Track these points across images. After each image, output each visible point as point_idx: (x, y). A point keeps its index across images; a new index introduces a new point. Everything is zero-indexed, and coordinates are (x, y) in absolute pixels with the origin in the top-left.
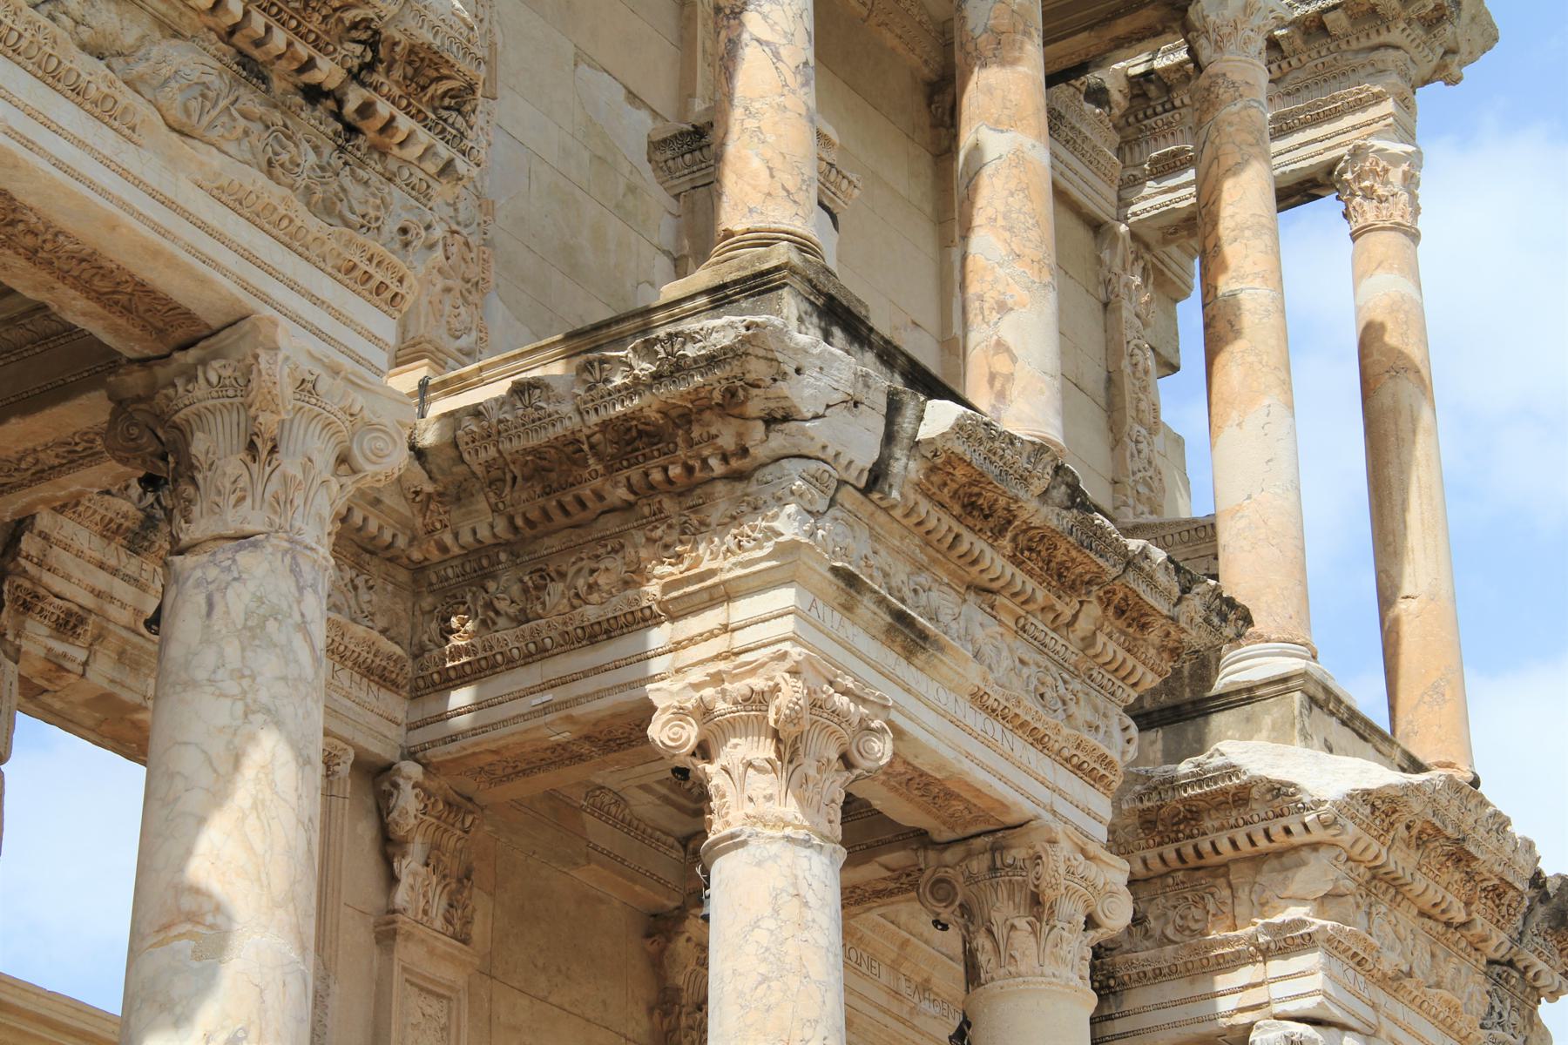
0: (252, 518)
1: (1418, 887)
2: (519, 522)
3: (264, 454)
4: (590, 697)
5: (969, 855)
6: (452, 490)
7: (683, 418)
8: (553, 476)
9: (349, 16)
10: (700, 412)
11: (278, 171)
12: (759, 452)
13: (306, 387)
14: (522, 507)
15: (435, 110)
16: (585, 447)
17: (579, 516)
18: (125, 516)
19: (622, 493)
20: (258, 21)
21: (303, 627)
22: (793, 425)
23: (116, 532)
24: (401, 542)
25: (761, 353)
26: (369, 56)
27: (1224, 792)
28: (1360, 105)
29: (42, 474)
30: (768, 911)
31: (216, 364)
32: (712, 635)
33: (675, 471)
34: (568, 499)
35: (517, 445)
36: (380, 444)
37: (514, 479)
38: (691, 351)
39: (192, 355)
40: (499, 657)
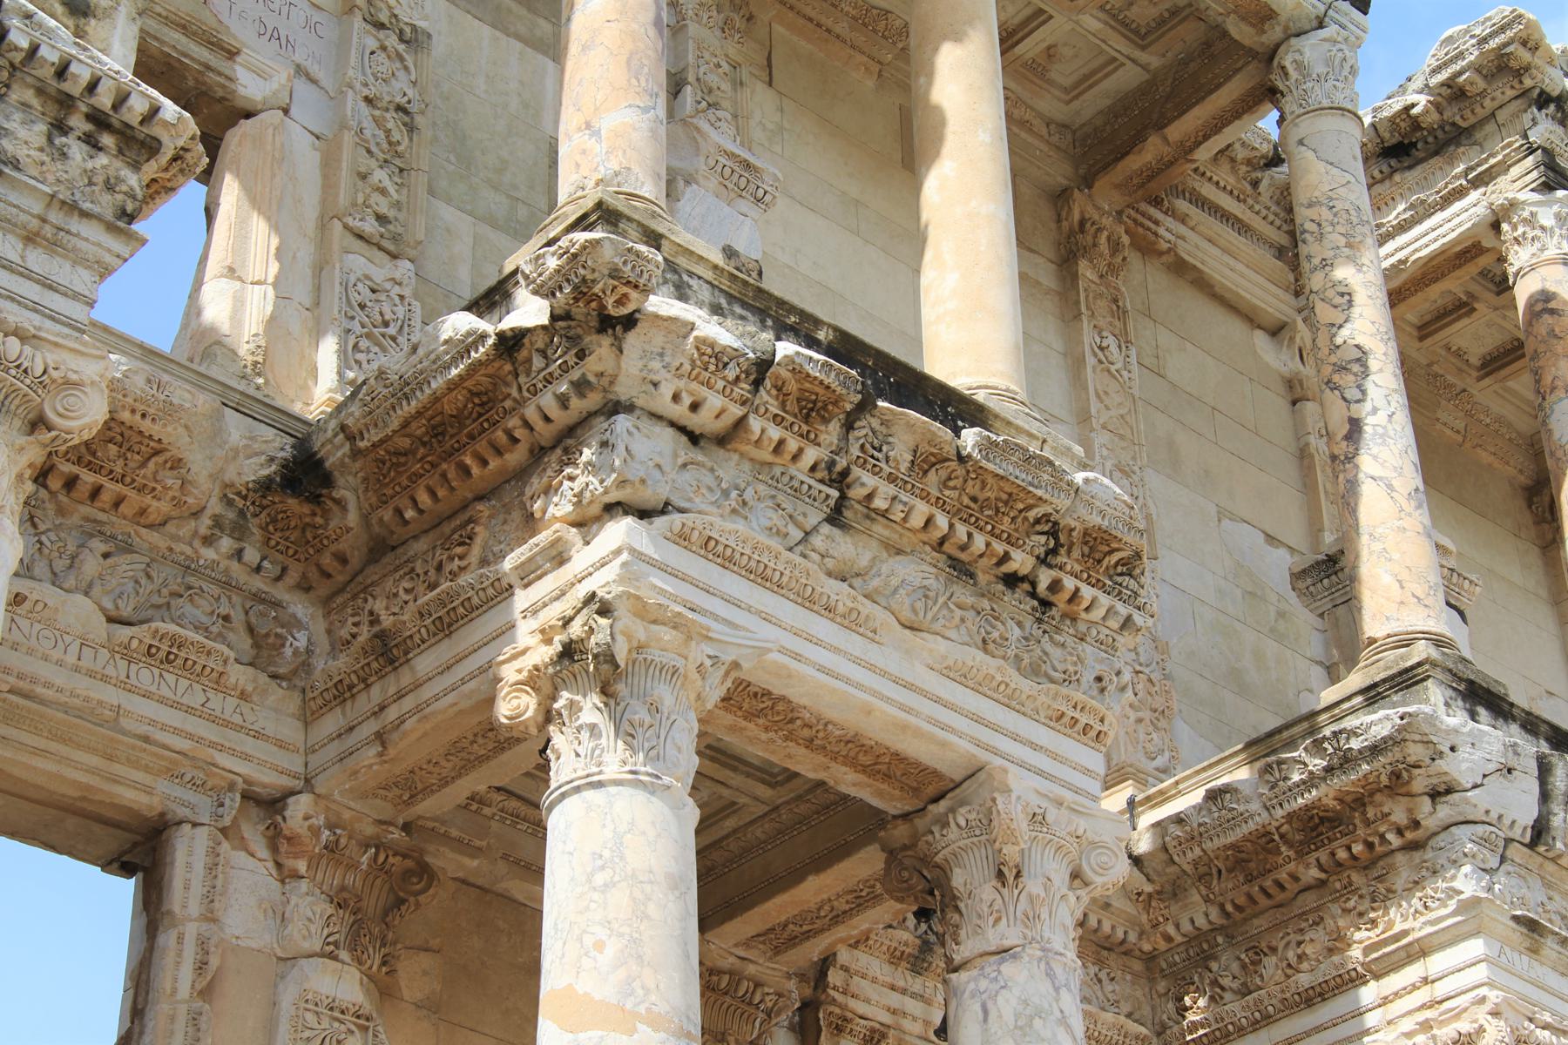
0: (1009, 934)
2: (1229, 908)
3: (1011, 880)
6: (1168, 888)
7: (1358, 802)
8: (1252, 865)
9: (1032, 515)
10: (1372, 794)
11: (991, 646)
12: (1430, 823)
13: (1038, 819)
14: (1230, 895)
15: (1110, 578)
16: (1276, 837)
17: (1280, 897)
18: (906, 944)
19: (1314, 873)
20: (961, 530)
21: (1063, 1021)
22: (1456, 796)
23: (900, 958)
24: (1132, 937)
25: (1417, 738)
26: (1052, 544)
29: (837, 919)
31: (963, 810)
32: (1414, 987)
33: (1357, 848)
34: (1268, 883)
35: (1218, 843)
36: (1104, 859)
38: (1355, 744)
39: (943, 805)
40: (1230, 1027)
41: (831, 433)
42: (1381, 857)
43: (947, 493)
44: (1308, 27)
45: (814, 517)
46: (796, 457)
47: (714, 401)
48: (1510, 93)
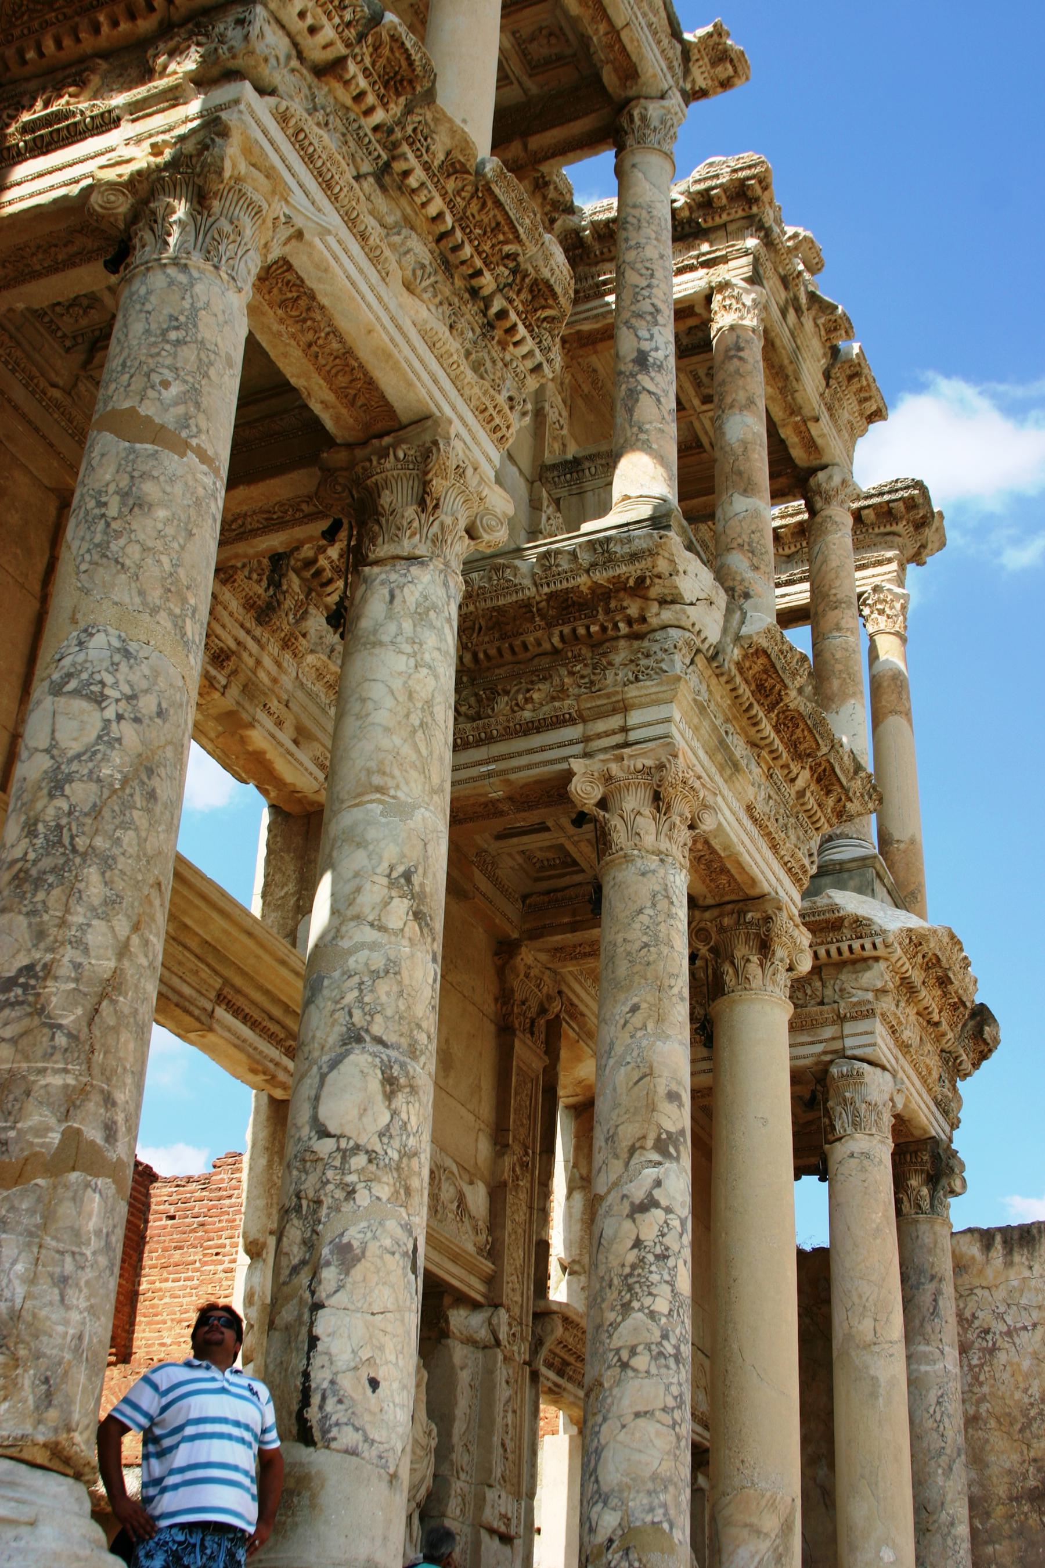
1: (924, 993)
2: (481, 656)
4: (520, 769)
5: (721, 915)
7: (603, 595)
8: (509, 628)
9: (507, 248)
10: (617, 591)
12: (654, 621)
14: (485, 646)
17: (522, 656)
18: (259, 597)
19: (556, 640)
20: (459, 234)
22: (678, 606)
23: (252, 607)
26: (510, 280)
27: (827, 921)
28: (879, 563)
30: (649, 904)
31: (404, 446)
33: (594, 629)
34: (517, 643)
36: (493, 523)
37: (480, 629)
41: (396, 109)
42: (607, 640)
43: (458, 199)
44: (653, 94)
45: (366, 167)
46: (369, 112)
47: (328, 33)
48: (741, 214)
